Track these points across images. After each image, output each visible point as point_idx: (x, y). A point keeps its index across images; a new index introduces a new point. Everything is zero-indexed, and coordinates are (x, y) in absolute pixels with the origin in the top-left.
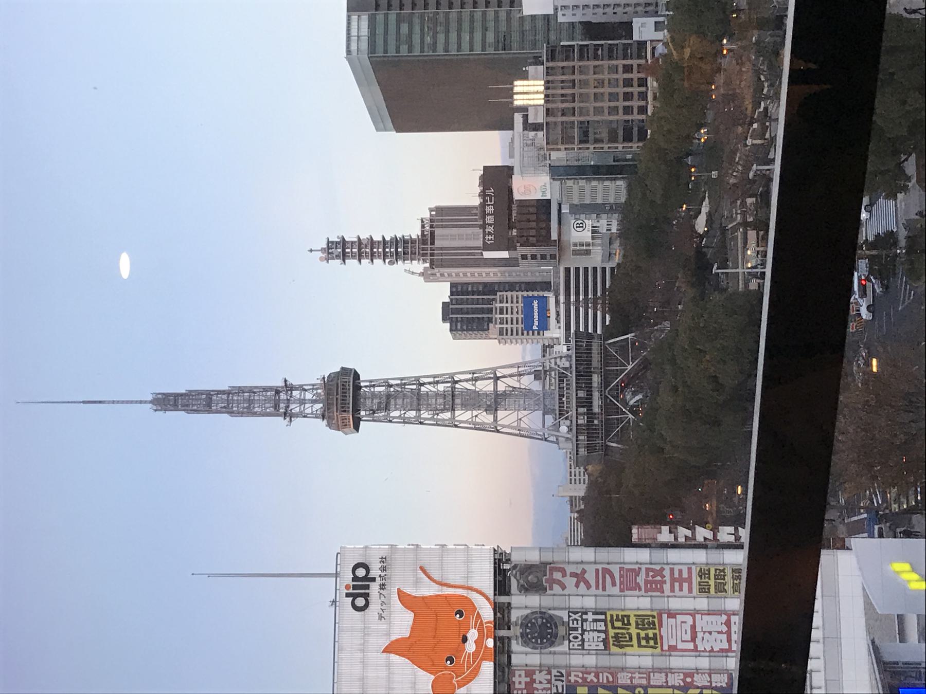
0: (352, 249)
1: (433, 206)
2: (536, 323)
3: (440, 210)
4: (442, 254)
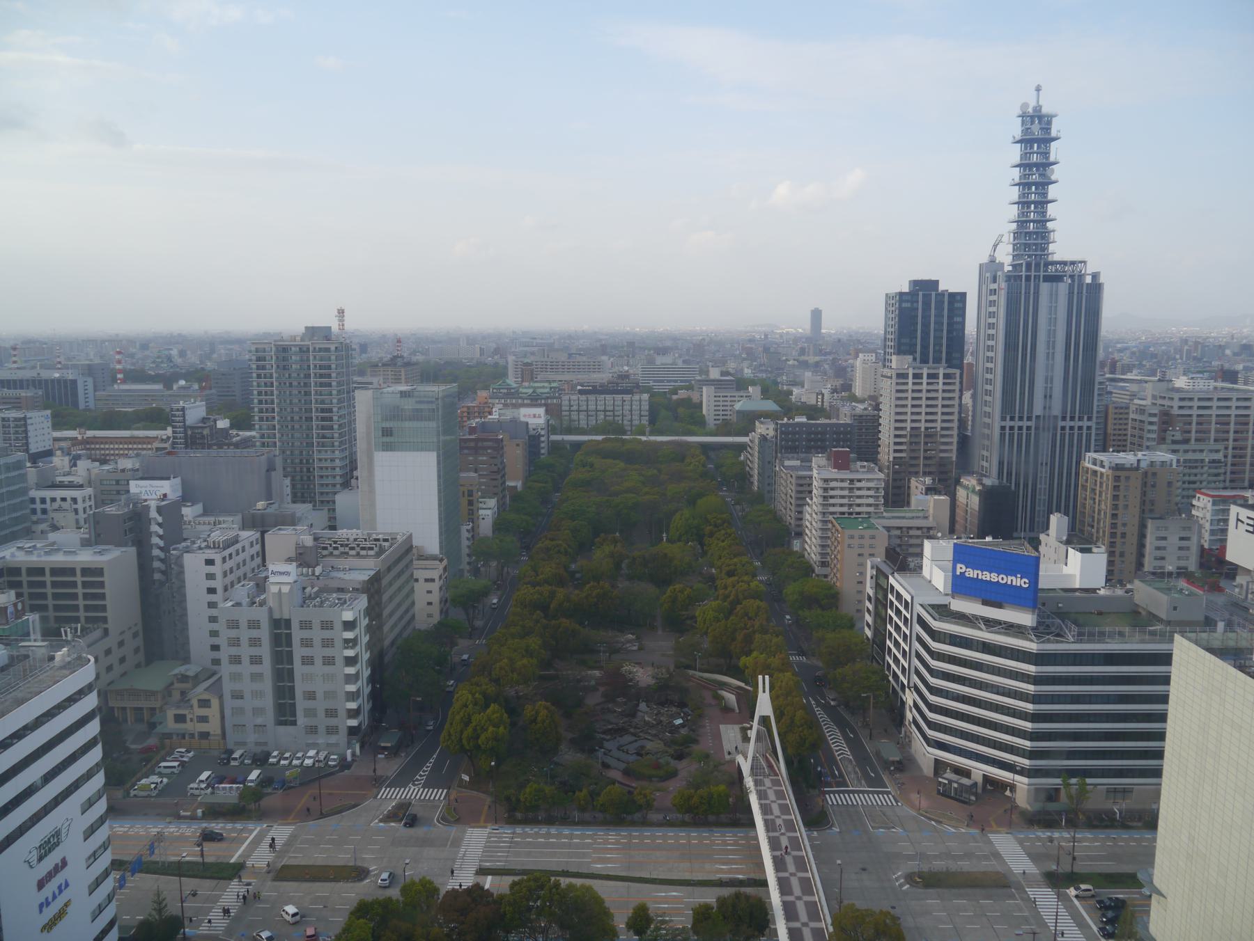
0: (1037, 153)
1: (1102, 280)
2: (971, 573)
3: (1096, 288)
4: (1027, 293)
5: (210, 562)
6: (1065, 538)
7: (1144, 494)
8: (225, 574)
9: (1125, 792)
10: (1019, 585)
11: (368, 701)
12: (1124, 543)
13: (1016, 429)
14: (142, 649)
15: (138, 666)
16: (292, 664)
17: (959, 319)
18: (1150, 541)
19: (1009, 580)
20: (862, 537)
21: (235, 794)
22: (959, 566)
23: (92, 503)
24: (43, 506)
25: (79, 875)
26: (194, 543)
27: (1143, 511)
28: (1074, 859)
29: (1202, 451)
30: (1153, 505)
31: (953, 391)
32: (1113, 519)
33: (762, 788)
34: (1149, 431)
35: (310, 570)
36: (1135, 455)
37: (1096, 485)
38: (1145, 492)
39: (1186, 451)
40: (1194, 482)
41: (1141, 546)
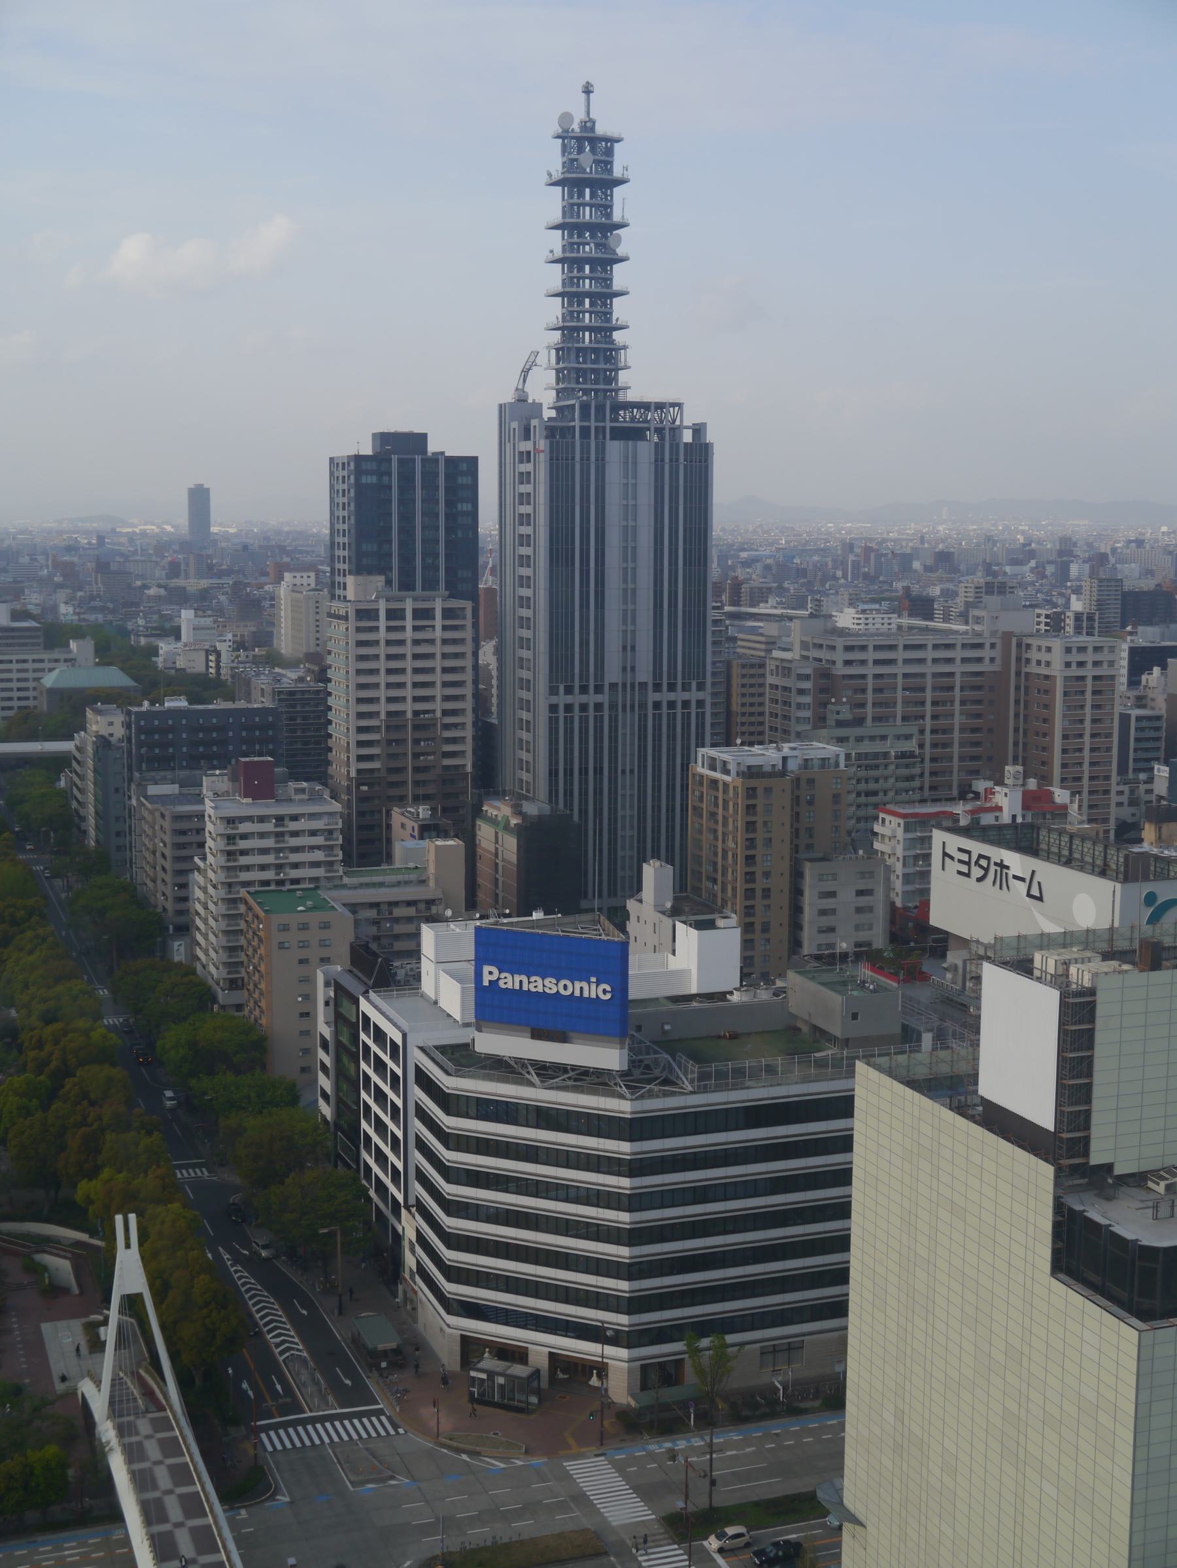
0: (591, 206)
1: (710, 437)
2: (510, 981)
4: (585, 459)
6: (669, 905)
7: (796, 817)
9: (791, 1349)
10: (593, 996)
12: (768, 907)
13: (577, 708)
17: (465, 507)
18: (810, 900)
19: (575, 988)
20: (304, 927)
22: (486, 969)
27: (796, 849)
28: (713, 1483)
29: (884, 738)
30: (811, 836)
31: (462, 641)
32: (747, 865)
33: (134, 1439)
34: (799, 706)
36: (779, 749)
37: (716, 805)
38: (797, 814)
39: (859, 739)
40: (875, 793)
41: (796, 910)
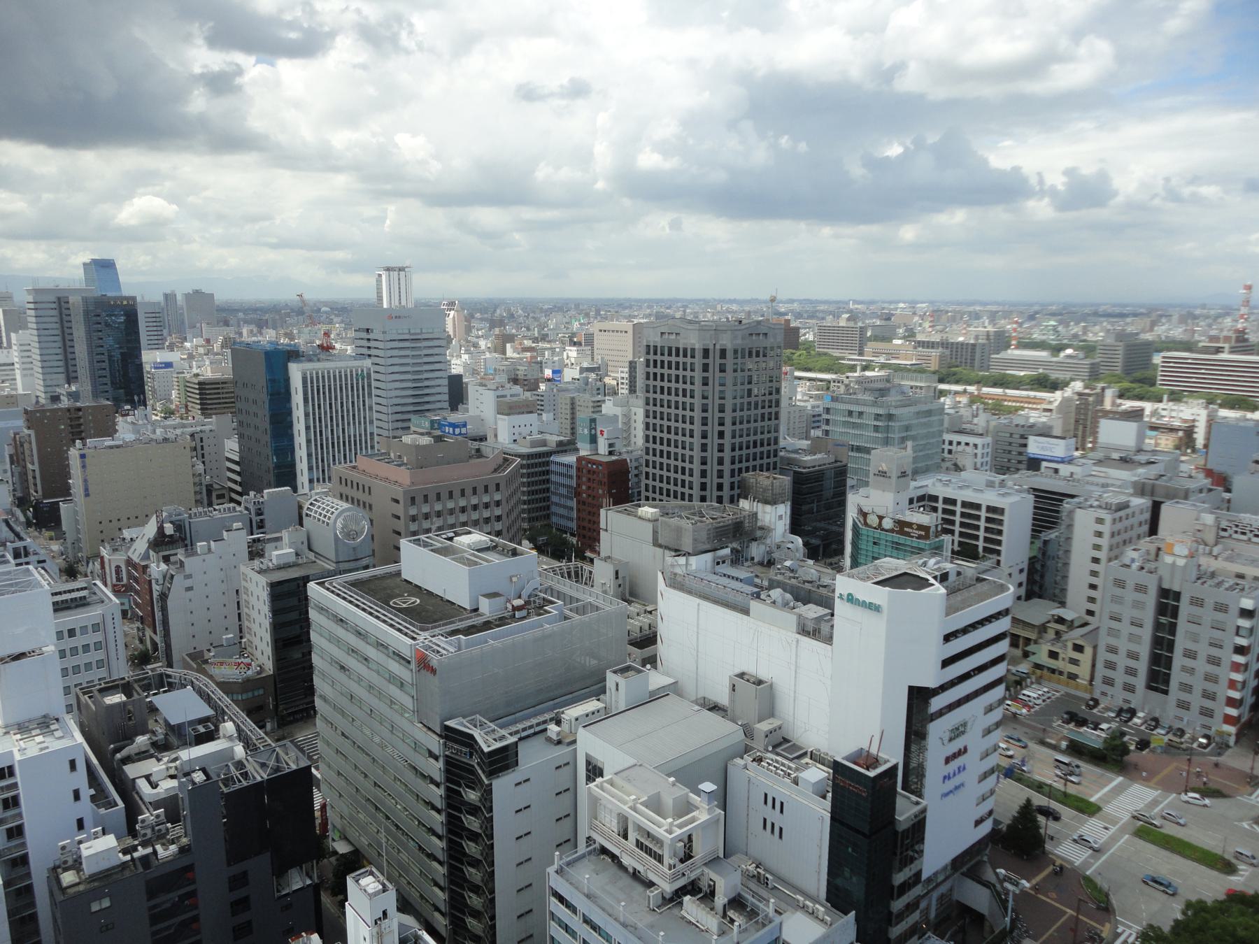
5: (1100, 521)
8: (1113, 535)
11: (1252, 695)
14: (1024, 584)
15: (1019, 598)
16: (1174, 635)
21: (1101, 741)
23: (989, 450)
24: (950, 447)
25: (974, 764)
26: (1086, 500)
35: (1208, 548)
